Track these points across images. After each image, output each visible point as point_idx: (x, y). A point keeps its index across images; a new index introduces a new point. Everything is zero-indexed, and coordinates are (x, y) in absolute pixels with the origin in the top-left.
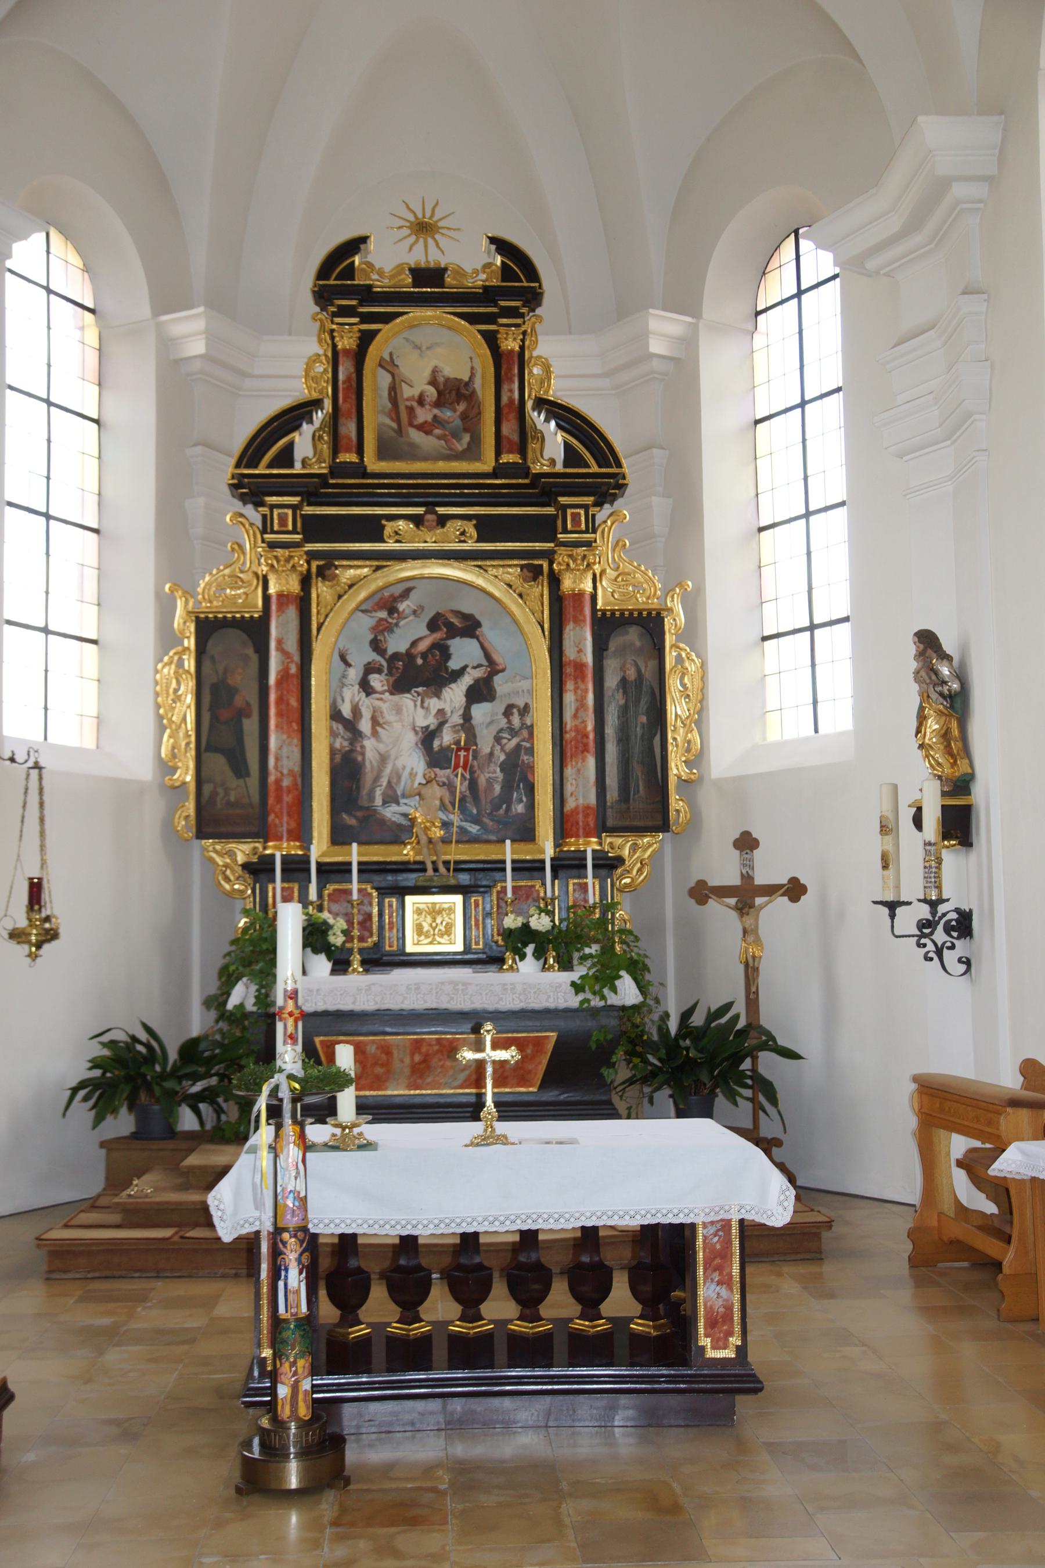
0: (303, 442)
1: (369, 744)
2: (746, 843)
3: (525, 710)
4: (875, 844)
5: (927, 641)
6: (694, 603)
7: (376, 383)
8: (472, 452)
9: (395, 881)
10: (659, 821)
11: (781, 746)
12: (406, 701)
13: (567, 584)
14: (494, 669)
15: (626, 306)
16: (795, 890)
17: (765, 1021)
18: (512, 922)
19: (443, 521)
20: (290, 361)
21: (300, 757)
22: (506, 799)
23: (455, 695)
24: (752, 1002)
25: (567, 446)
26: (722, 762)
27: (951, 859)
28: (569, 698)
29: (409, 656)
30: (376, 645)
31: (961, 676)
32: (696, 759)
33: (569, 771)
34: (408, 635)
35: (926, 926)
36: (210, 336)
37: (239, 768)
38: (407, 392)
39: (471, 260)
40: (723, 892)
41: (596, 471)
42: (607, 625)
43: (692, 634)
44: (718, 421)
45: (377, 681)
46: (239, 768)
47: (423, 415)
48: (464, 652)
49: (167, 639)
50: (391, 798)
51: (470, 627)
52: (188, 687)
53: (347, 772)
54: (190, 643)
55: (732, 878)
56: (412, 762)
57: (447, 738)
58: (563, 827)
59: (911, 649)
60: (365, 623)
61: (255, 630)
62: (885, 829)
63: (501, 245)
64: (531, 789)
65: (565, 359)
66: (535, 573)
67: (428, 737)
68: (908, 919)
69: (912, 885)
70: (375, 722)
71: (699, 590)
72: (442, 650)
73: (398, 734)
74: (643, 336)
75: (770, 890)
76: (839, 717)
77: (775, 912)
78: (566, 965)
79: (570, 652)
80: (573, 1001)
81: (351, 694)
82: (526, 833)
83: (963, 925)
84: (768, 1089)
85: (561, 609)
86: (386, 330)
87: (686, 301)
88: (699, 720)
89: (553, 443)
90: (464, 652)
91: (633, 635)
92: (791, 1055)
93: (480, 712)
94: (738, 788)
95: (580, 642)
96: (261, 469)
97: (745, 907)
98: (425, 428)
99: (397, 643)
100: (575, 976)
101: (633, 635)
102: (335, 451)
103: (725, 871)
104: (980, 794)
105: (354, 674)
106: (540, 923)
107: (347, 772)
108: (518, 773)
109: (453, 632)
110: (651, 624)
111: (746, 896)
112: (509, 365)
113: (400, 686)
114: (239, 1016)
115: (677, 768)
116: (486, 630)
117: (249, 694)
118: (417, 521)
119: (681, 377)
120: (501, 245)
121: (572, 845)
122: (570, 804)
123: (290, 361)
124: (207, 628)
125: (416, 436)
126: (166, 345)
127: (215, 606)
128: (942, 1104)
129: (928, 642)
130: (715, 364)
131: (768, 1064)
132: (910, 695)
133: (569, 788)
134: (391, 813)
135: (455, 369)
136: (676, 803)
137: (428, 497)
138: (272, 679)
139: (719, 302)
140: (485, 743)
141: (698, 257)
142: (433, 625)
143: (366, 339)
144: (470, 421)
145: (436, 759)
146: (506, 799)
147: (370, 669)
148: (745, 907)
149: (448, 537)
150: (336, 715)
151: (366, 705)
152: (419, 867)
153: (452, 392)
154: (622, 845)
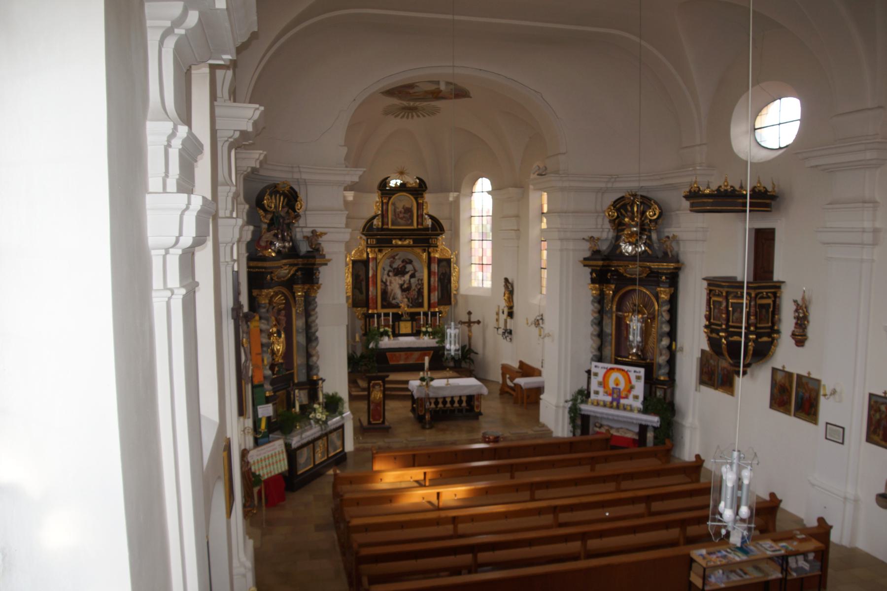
0: (375, 222)
1: (389, 288)
2: (470, 313)
3: (422, 280)
4: (495, 317)
5: (506, 280)
6: (457, 256)
7: (390, 207)
8: (412, 224)
9: (397, 318)
10: (449, 303)
11: (475, 288)
12: (397, 278)
13: (432, 255)
14: (415, 271)
15: (444, 189)
16: (479, 322)
17: (472, 348)
18: (424, 329)
19: (405, 239)
20: (372, 204)
21: (375, 292)
22: (418, 298)
23: (407, 277)
24: (470, 344)
25: (433, 224)
26: (463, 290)
27: (509, 320)
28: (432, 279)
29: (397, 269)
30: (391, 266)
31: (512, 287)
32: (457, 290)
33: (432, 295)
34: (398, 264)
35: (504, 333)
36: (354, 197)
37: (361, 293)
38: (398, 210)
39: (412, 181)
40: (464, 323)
41: (437, 227)
42: (440, 261)
43: (457, 263)
44: (463, 216)
45: (391, 274)
46: (361, 293)
47: (401, 215)
48: (409, 267)
49: (347, 264)
50: (394, 299)
51: (410, 262)
52: (350, 276)
53: (385, 293)
54: (351, 265)
55: (467, 320)
56: (398, 292)
57: (405, 286)
58: (430, 306)
59: (503, 281)
60: (388, 262)
61: (366, 263)
62: (498, 314)
63: (418, 178)
64: (423, 296)
65: (432, 204)
66: (424, 251)
67: (401, 286)
68: (501, 331)
69: (502, 325)
70: (391, 282)
71: (459, 254)
72: (404, 267)
73: (395, 284)
74: (448, 197)
75: (474, 322)
76: (488, 284)
77: (475, 327)
78: (434, 338)
79: (432, 269)
80: (437, 345)
81: (385, 277)
82: (421, 305)
83: (510, 332)
84: (472, 361)
85: (430, 260)
86: (394, 197)
87: (457, 189)
88: (458, 281)
89: (429, 222)
90: (409, 267)
91: (444, 263)
92: (476, 353)
93: (413, 280)
94: (466, 297)
95: (435, 267)
96: (368, 230)
97: (469, 326)
98: (401, 218)
99: (395, 266)
100: (437, 340)
101: (444, 263)
102: (383, 224)
103: (465, 318)
104: (515, 309)
105: (386, 272)
106: (430, 330)
107: (385, 293)
108: (420, 292)
109: (407, 263)
110: (448, 261)
111: (469, 323)
112: (420, 206)
113: (396, 275)
114: (372, 349)
115: (454, 292)
116: (415, 263)
117: (363, 276)
118: (400, 239)
119: (455, 207)
120: (418, 178)
121: (432, 310)
122: (432, 301)
123: (372, 204)
124: (354, 262)
125: (399, 220)
126: (344, 197)
127: (357, 258)
128: (505, 369)
129: (506, 280)
130: (463, 203)
131: (472, 356)
132: (503, 289)
133: (432, 298)
134: (394, 302)
135: (408, 206)
136: (453, 299)
137: (402, 234)
138: (370, 275)
139: (464, 190)
140: (413, 287)
141: (461, 185)
142: (403, 262)
143: (390, 198)
144: (411, 217)
145: (403, 290)
146: (418, 298)
147: (389, 271)
148: (469, 326)
149: (406, 242)
150: (382, 281)
151: (389, 279)
152: (402, 315)
153: (408, 211)
154: (442, 308)
